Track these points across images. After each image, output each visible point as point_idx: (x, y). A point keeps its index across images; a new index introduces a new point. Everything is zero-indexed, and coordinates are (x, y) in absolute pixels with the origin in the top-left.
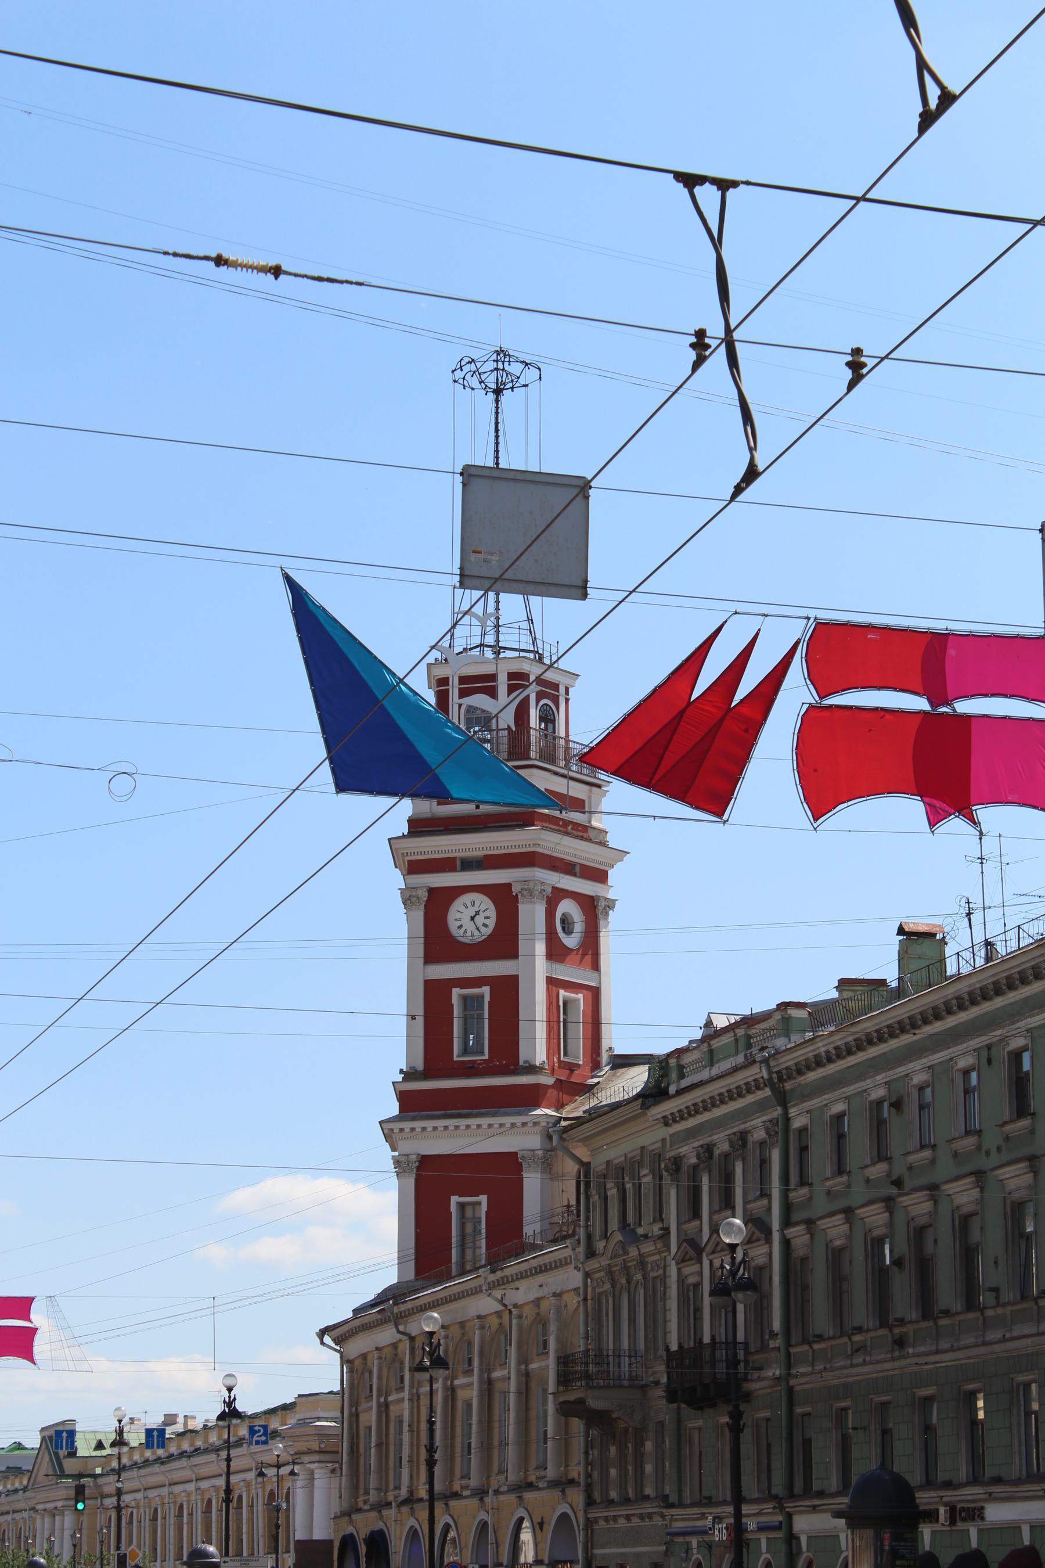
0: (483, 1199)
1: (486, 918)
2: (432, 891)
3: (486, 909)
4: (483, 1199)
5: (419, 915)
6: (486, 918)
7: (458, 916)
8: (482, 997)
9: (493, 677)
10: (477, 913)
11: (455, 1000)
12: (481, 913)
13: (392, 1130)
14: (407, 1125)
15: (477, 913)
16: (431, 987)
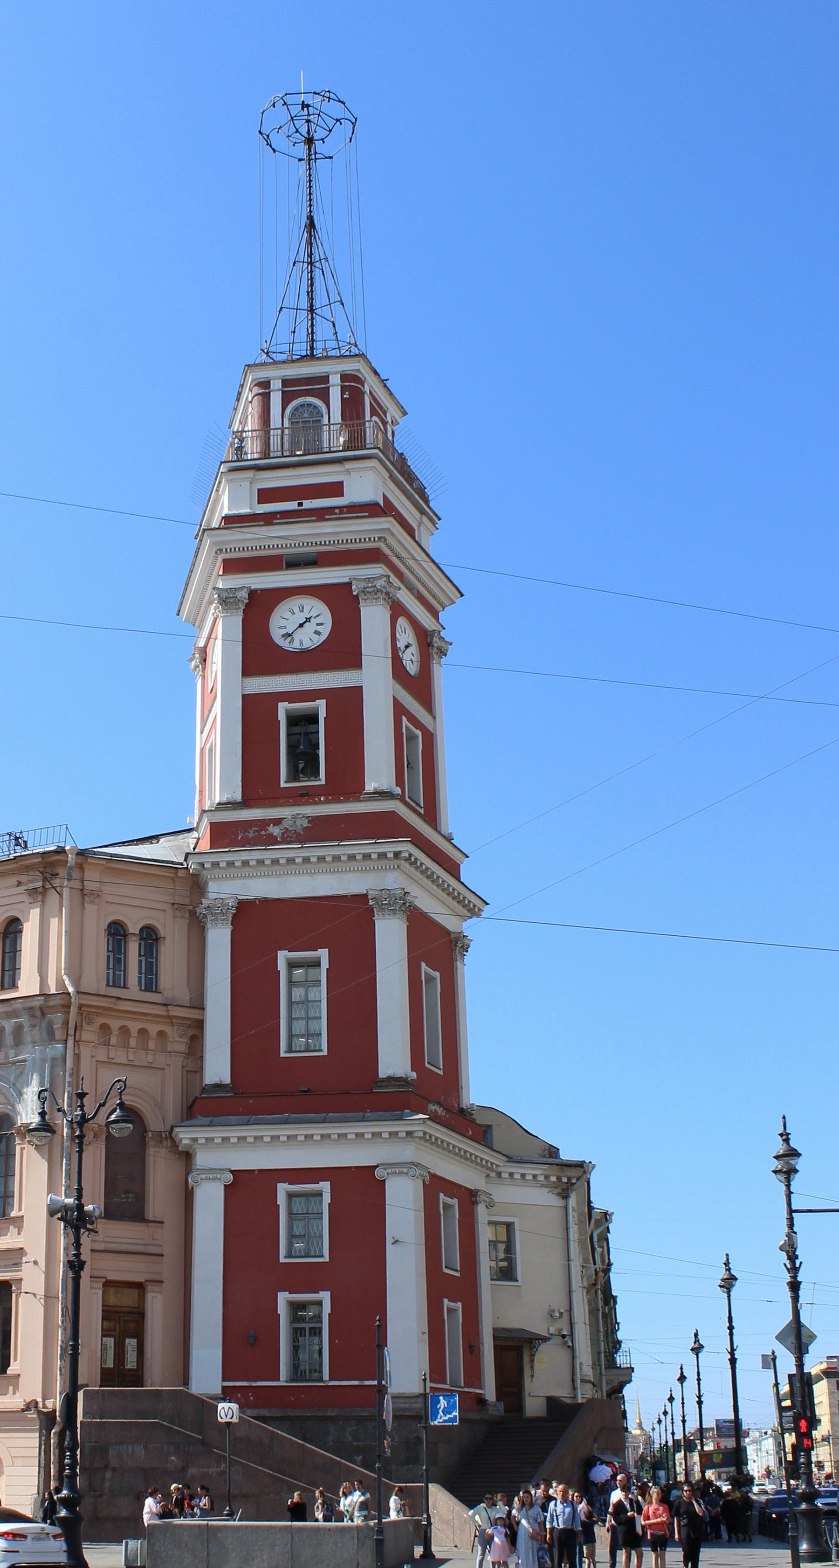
0: (323, 954)
1: (318, 624)
2: (253, 594)
3: (319, 615)
4: (323, 954)
5: (237, 620)
6: (318, 624)
7: (283, 623)
8: (313, 719)
9: (325, 379)
10: (308, 620)
11: (282, 717)
12: (312, 620)
13: (202, 865)
14: (223, 859)
15: (308, 620)
16: (248, 701)
